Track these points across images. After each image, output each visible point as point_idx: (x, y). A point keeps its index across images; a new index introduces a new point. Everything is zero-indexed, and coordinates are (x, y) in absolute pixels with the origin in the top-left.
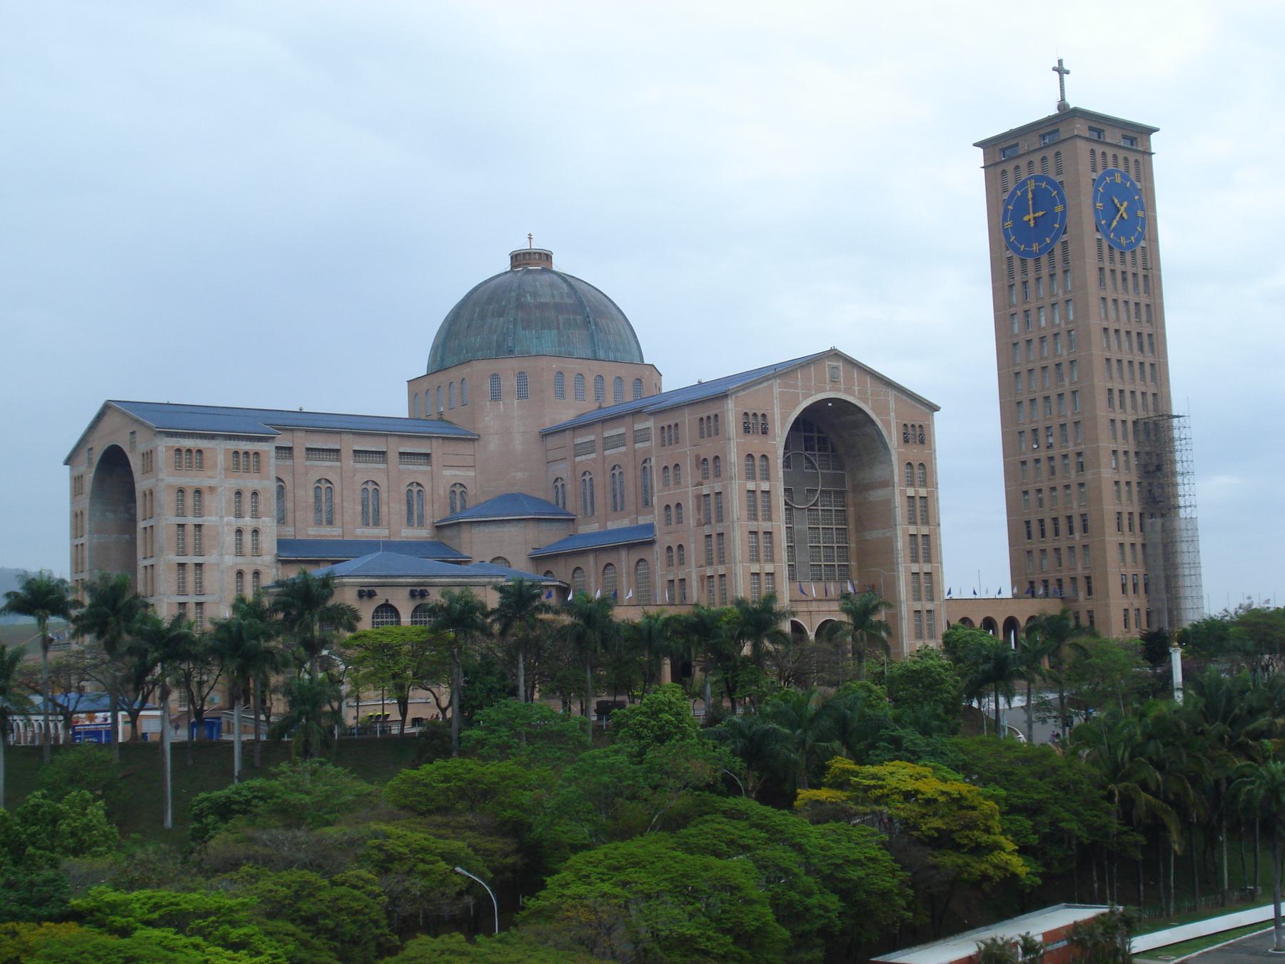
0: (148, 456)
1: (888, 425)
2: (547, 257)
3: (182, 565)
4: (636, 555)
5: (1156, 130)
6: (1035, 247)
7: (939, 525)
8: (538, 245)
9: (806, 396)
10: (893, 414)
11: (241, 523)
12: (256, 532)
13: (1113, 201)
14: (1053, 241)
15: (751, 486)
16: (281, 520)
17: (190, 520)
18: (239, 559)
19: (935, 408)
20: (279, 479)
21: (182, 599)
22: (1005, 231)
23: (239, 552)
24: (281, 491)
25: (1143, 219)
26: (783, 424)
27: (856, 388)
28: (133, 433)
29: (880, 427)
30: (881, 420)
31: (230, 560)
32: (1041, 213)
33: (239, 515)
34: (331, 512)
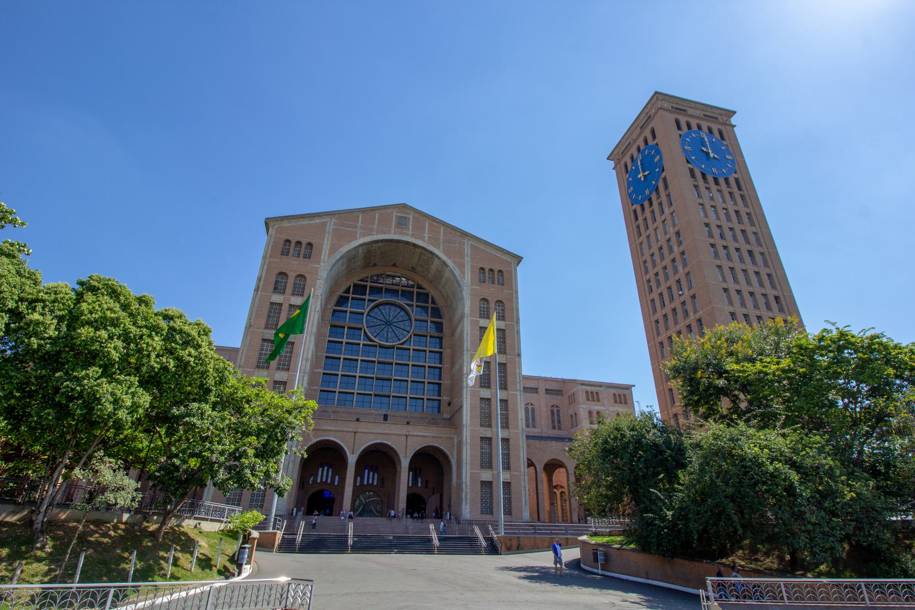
1: (461, 266)
5: (734, 113)
6: (647, 192)
7: (519, 355)
9: (364, 235)
10: (467, 259)
13: (703, 151)
14: (657, 182)
15: (277, 298)
19: (519, 259)
22: (630, 195)
25: (733, 162)
26: (333, 250)
27: (426, 235)
29: (451, 267)
30: (454, 262)
32: (647, 173)
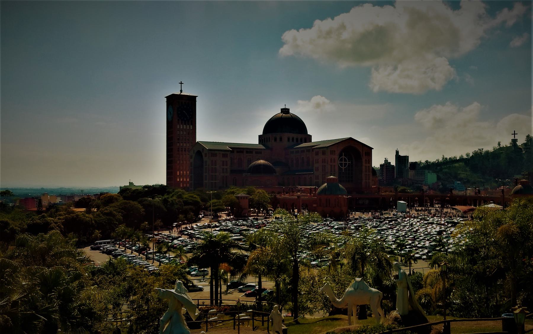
2: (289, 109)
8: (287, 107)
33: (223, 165)
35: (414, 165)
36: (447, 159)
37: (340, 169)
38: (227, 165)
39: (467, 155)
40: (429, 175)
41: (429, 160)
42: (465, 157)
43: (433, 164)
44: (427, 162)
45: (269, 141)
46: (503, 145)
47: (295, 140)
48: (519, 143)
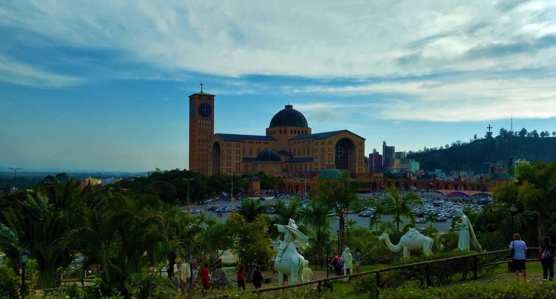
0: (222, 144)
2: (292, 106)
3: (227, 162)
4: (300, 164)
8: (290, 104)
11: (237, 155)
12: (239, 157)
16: (243, 155)
17: (229, 155)
18: (237, 161)
20: (243, 148)
21: (228, 167)
23: (237, 160)
24: (244, 149)
28: (220, 140)
31: (236, 162)
34: (252, 153)
35: (399, 154)
36: (428, 150)
37: (336, 157)
38: (239, 154)
39: (447, 146)
40: (413, 163)
41: (413, 151)
42: (444, 148)
43: (417, 154)
44: (410, 152)
45: (275, 133)
46: (479, 137)
47: (297, 132)
48: (494, 136)
